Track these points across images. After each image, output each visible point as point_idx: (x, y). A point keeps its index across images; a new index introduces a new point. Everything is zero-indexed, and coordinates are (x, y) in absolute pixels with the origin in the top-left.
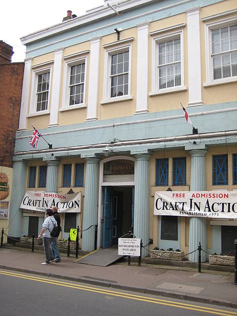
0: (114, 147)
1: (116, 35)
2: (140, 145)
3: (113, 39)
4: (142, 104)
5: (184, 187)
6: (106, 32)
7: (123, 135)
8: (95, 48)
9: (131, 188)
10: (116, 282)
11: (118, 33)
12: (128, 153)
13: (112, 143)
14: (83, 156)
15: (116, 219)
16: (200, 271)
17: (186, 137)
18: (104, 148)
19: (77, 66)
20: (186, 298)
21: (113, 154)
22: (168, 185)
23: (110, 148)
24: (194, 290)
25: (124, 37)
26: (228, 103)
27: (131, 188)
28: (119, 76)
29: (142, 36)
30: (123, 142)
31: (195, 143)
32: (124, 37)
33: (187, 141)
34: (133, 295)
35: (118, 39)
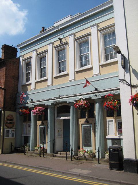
0: (60, 99)
1: (59, 41)
2: (71, 98)
3: (58, 43)
4: (71, 77)
5: (93, 118)
6: (55, 40)
7: (63, 93)
8: (50, 48)
9: (69, 120)
10: (52, 168)
11: (61, 40)
12: (66, 102)
13: (59, 97)
14: (46, 104)
15: (14, 137)
16: (99, 163)
17: (92, 92)
18: (54, 100)
19: (42, 58)
20: (79, 176)
21: (60, 103)
22: (85, 118)
23: (58, 100)
24: (85, 172)
25: (64, 41)
26: (111, 73)
27: (69, 120)
28: (62, 62)
29: (71, 40)
30: (64, 97)
31: (96, 95)
32: (64, 41)
33: (93, 95)
34: (76, 179)
35: (61, 43)
